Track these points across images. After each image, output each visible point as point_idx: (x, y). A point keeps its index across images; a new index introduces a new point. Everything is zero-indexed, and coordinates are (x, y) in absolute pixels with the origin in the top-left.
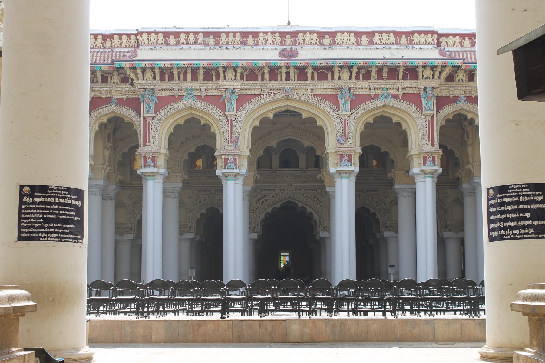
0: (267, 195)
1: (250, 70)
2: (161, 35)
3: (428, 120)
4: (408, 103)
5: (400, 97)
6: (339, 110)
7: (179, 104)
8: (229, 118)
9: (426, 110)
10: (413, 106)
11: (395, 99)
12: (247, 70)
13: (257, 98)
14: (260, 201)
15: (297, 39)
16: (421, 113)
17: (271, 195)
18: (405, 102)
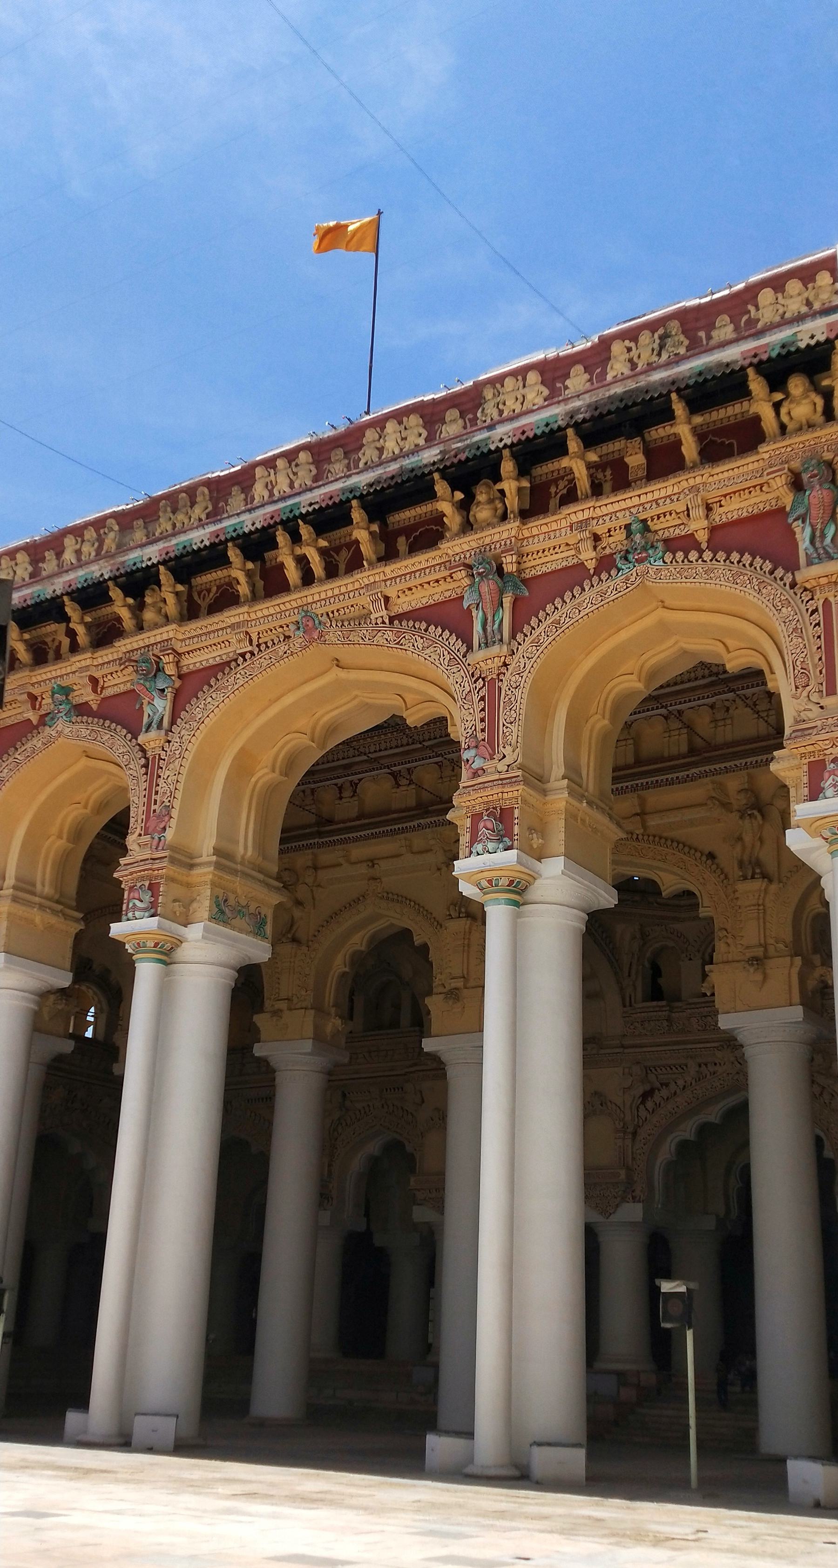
0: (667, 1085)
1: (218, 587)
2: (21, 557)
3: (826, 602)
4: (735, 556)
5: (702, 537)
6: (470, 648)
7: (35, 741)
8: (149, 754)
9: (810, 563)
10: (758, 561)
11: (680, 555)
12: (209, 591)
13: (227, 670)
14: (650, 1104)
15: (360, 455)
16: (793, 585)
17: (681, 1083)
18: (721, 555)
